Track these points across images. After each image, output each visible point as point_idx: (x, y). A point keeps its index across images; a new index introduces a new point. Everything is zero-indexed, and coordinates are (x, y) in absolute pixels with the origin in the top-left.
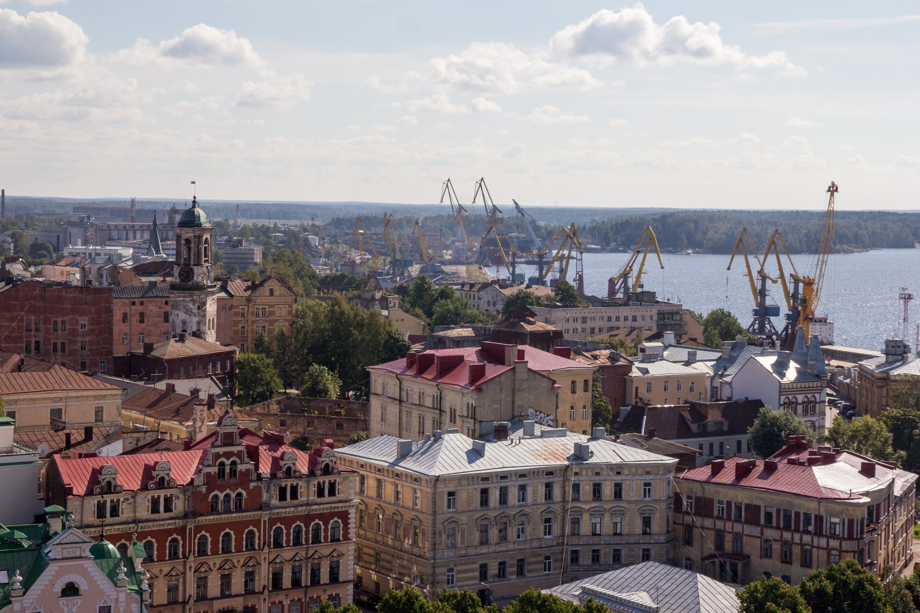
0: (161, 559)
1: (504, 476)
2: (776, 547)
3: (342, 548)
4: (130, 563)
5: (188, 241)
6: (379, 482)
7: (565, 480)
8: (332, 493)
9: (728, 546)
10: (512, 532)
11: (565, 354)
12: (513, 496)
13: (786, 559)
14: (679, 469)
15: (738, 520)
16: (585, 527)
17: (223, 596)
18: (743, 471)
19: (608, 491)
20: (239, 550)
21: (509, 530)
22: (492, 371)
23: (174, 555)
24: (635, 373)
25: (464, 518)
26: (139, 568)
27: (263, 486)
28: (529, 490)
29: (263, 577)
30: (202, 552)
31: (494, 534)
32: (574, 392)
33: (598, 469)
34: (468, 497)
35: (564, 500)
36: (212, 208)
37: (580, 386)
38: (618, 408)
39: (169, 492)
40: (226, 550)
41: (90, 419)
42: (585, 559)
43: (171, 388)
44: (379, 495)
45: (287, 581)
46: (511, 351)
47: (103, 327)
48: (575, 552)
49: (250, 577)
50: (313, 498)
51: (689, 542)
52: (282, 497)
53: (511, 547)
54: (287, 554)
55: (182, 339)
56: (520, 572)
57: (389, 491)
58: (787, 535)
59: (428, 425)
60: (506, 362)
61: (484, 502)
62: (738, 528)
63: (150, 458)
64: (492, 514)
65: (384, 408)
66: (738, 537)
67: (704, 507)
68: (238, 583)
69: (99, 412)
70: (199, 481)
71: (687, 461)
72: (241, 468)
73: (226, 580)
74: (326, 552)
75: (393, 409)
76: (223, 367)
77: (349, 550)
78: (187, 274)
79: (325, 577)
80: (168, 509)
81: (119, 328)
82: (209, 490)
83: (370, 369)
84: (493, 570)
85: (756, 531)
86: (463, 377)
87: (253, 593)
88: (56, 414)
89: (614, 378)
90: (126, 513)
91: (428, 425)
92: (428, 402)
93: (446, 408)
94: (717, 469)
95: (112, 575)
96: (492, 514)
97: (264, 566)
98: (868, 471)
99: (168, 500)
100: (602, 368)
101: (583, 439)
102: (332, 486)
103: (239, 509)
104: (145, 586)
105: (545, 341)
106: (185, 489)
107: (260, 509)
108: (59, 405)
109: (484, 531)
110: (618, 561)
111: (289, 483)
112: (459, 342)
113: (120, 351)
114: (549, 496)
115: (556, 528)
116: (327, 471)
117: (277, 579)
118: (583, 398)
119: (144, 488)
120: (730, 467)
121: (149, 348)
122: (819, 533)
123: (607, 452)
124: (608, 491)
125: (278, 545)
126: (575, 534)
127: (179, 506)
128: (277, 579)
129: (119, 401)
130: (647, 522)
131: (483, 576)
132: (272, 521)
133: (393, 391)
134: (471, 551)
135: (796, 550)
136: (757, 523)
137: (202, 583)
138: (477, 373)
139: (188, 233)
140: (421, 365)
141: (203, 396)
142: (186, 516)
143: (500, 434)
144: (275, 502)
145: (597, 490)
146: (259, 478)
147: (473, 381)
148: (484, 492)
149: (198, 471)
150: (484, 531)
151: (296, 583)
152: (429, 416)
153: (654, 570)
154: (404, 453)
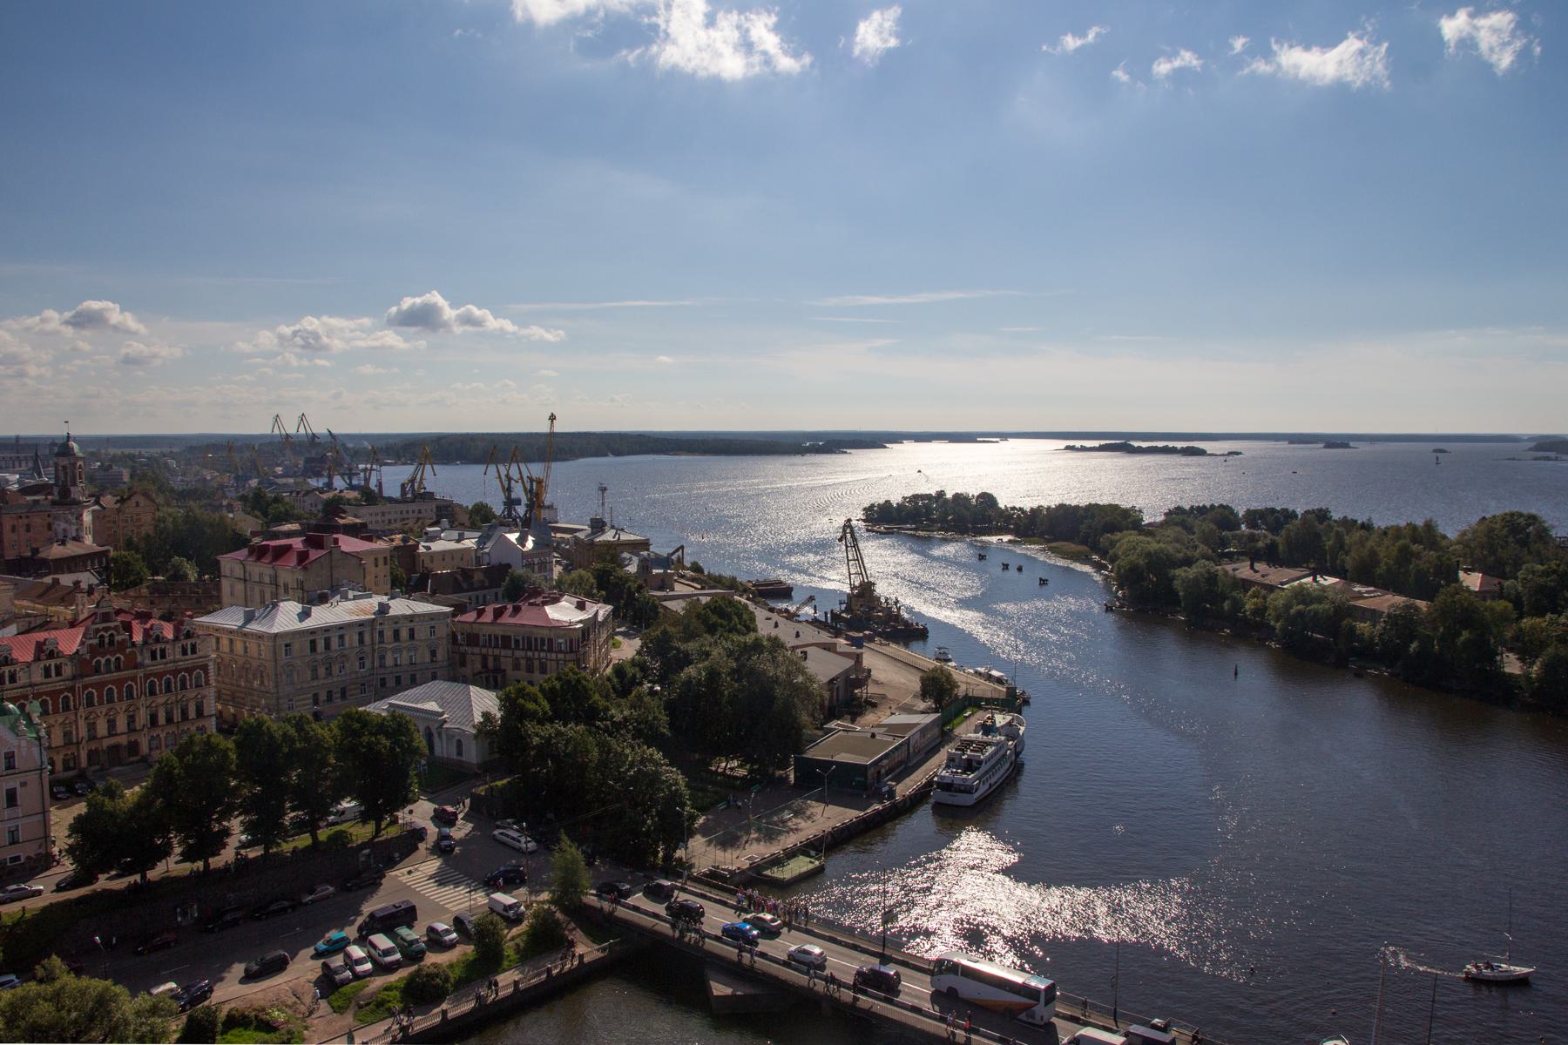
0: (56, 711)
1: (327, 629)
2: (523, 662)
3: (205, 692)
4: (29, 718)
5: (64, 467)
6: (231, 641)
8: (194, 652)
9: (491, 665)
10: (336, 669)
11: (369, 539)
12: (335, 643)
13: (530, 670)
14: (454, 615)
15: (496, 646)
16: (389, 662)
17: (110, 735)
18: (498, 613)
19: (404, 634)
20: (120, 699)
22: (314, 554)
23: (67, 708)
24: (422, 550)
26: (37, 720)
28: (347, 639)
29: (142, 718)
30: (90, 703)
31: (322, 671)
33: (396, 619)
34: (300, 647)
35: (373, 643)
36: (82, 441)
37: (381, 562)
38: (410, 575)
39: (58, 661)
40: (110, 700)
42: (391, 683)
43: (56, 582)
44: (232, 651)
45: (162, 719)
46: (328, 538)
48: (383, 680)
49: (131, 719)
50: (179, 656)
51: (463, 664)
52: (154, 657)
54: (161, 700)
55: (63, 543)
57: (239, 647)
58: (530, 654)
59: (268, 596)
62: (497, 651)
63: (41, 636)
64: (319, 658)
65: (232, 587)
66: (497, 658)
67: (473, 639)
68: (122, 724)
70: (84, 651)
71: (460, 609)
72: (118, 638)
73: (112, 724)
75: (240, 587)
76: (100, 563)
77: (210, 693)
78: (65, 493)
79: (192, 714)
80: (58, 673)
82: (92, 658)
84: (323, 696)
85: (509, 653)
87: (135, 730)
89: (407, 555)
90: (22, 679)
91: (268, 596)
92: (267, 580)
93: (281, 582)
94: (481, 613)
95: (14, 728)
96: (319, 658)
97: (143, 711)
98: (581, 606)
99: (58, 668)
100: (396, 548)
101: (384, 599)
102: (194, 647)
103: (118, 669)
104: (43, 733)
105: (353, 531)
106: (71, 658)
107: (136, 667)
109: (315, 670)
110: (414, 682)
111: (158, 647)
112: (289, 534)
113: (10, 554)
114: (361, 641)
115: (368, 664)
116: (189, 635)
118: (383, 570)
119: (37, 659)
120: (490, 610)
121: (36, 551)
122: (550, 650)
123: (401, 607)
124: (404, 634)
125: (152, 693)
126: (382, 666)
129: (11, 594)
130: (433, 653)
131: (316, 702)
132: (147, 677)
133: (239, 572)
135: (536, 663)
136: (509, 647)
137: (92, 727)
138: (302, 557)
139: (64, 462)
140: (260, 553)
141: (84, 586)
142: (74, 678)
143: (323, 599)
144: (148, 661)
145: (396, 634)
146: (134, 645)
147: (300, 562)
148: (313, 643)
149: (82, 643)
150: (315, 670)
151: (169, 720)
152: (268, 591)
153: (440, 686)
154: (249, 618)
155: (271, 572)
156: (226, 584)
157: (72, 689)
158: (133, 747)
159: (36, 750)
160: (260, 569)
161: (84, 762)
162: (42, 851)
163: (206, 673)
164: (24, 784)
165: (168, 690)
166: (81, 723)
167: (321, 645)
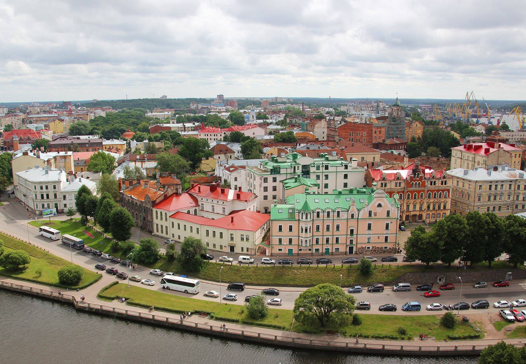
3: (447, 200)
6: (458, 181)
7: (516, 184)
8: (445, 184)
10: (498, 198)
12: (499, 187)
21: (497, 197)
22: (492, 150)
25: (484, 194)
27: (426, 181)
28: (504, 186)
29: (425, 206)
30: (408, 198)
31: (492, 198)
32: (515, 157)
34: (486, 187)
37: (518, 156)
40: (415, 198)
41: (372, 161)
42: (520, 207)
43: (392, 152)
45: (431, 208)
46: (496, 145)
47: (370, 135)
50: (440, 185)
52: (431, 184)
53: (497, 203)
54: (432, 201)
56: (499, 210)
57: (460, 184)
60: (495, 147)
61: (490, 189)
64: (492, 193)
69: (374, 158)
73: (415, 206)
74: (443, 200)
75: (459, 160)
76: (404, 147)
77: (449, 201)
79: (442, 208)
81: (374, 135)
82: (411, 181)
83: (452, 148)
86: (482, 152)
88: (363, 158)
90: (388, 186)
92: (470, 159)
93: (476, 160)
97: (425, 203)
99: (400, 183)
101: (521, 172)
102: (446, 182)
104: (399, 206)
106: (404, 180)
108: (363, 156)
109: (489, 197)
111: (433, 180)
113: (374, 142)
114: (510, 188)
116: (444, 177)
117: (429, 207)
121: (384, 141)
125: (429, 197)
127: (403, 185)
128: (429, 207)
129: (379, 155)
132: (428, 191)
134: (485, 203)
138: (487, 151)
140: (469, 148)
141: (402, 155)
143: (496, 169)
144: (429, 185)
146: (425, 178)
148: (490, 186)
150: (489, 197)
151: (434, 209)
152: (470, 163)
154: (466, 173)
155: (473, 156)
156: (453, 159)
157: (403, 192)
158: (420, 216)
159: (396, 211)
160: (469, 155)
161: (404, 219)
162: (394, 247)
163: (449, 193)
164: (391, 222)
165: (435, 197)
166: (405, 204)
167: (493, 187)
